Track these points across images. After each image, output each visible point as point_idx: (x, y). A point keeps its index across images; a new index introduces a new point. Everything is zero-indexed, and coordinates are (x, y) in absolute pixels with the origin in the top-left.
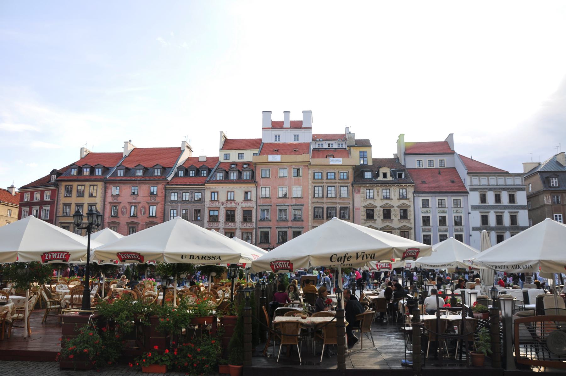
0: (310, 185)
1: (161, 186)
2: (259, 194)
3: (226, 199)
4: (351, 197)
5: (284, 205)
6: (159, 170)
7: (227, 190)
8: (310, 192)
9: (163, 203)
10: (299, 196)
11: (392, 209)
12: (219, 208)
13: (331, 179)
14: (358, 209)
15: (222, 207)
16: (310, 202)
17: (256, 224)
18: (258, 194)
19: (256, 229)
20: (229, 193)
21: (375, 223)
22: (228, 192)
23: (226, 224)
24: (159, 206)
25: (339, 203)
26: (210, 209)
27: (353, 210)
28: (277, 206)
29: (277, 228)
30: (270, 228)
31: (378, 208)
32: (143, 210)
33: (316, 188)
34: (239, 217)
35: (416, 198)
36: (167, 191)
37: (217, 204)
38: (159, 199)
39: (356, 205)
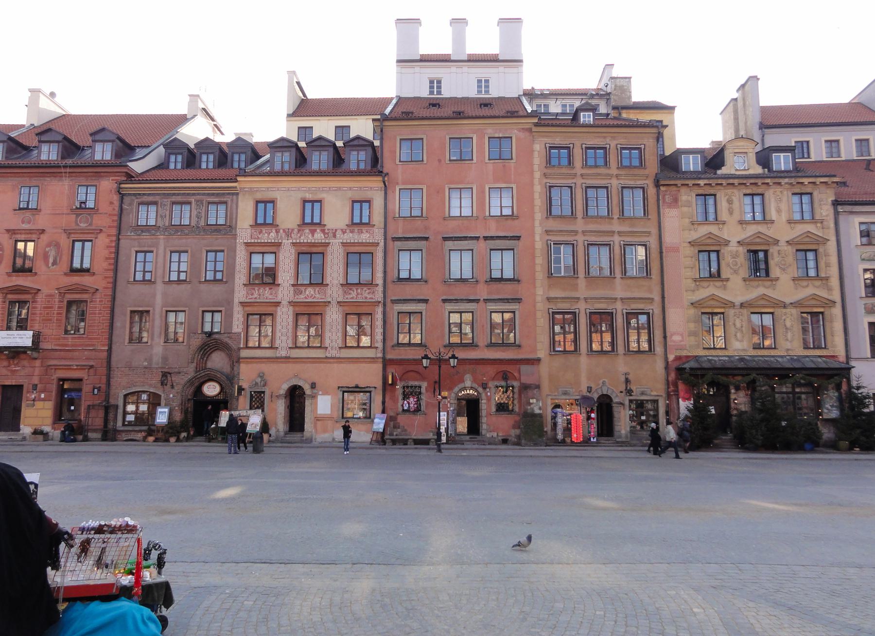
0: (536, 181)
1: (107, 184)
2: (394, 206)
3: (298, 221)
4: (653, 215)
5: (465, 238)
6: (108, 147)
7: (300, 195)
8: (539, 202)
9: (114, 231)
10: (507, 212)
11: (773, 250)
12: (278, 245)
13: (596, 166)
14: (676, 250)
15: (287, 242)
16: (538, 230)
17: (384, 292)
18: (390, 206)
19: (384, 305)
20: (308, 206)
21: (725, 288)
22: (305, 201)
23: (297, 292)
24: (103, 241)
25: (620, 233)
26: (253, 248)
27: (661, 253)
28: (445, 239)
29: (444, 301)
30: (426, 301)
31: (733, 247)
32: (52, 254)
33: (555, 193)
34: (335, 271)
35: (841, 218)
36: (127, 200)
37: (273, 234)
38: (102, 221)
39: (669, 239)
